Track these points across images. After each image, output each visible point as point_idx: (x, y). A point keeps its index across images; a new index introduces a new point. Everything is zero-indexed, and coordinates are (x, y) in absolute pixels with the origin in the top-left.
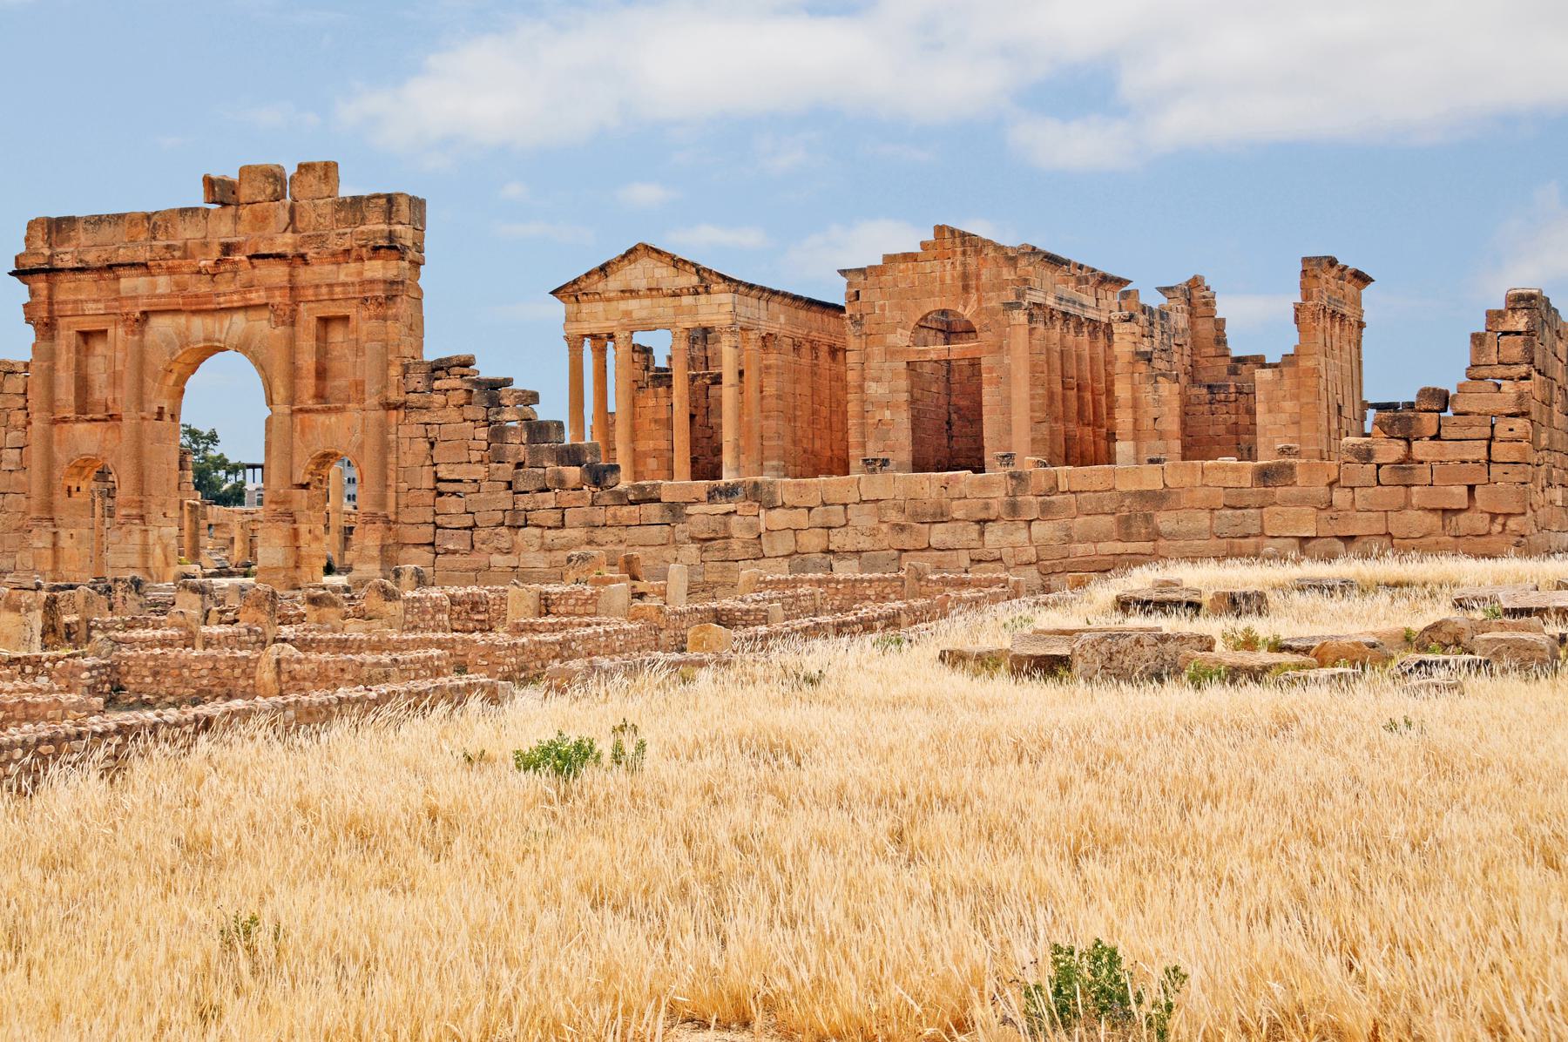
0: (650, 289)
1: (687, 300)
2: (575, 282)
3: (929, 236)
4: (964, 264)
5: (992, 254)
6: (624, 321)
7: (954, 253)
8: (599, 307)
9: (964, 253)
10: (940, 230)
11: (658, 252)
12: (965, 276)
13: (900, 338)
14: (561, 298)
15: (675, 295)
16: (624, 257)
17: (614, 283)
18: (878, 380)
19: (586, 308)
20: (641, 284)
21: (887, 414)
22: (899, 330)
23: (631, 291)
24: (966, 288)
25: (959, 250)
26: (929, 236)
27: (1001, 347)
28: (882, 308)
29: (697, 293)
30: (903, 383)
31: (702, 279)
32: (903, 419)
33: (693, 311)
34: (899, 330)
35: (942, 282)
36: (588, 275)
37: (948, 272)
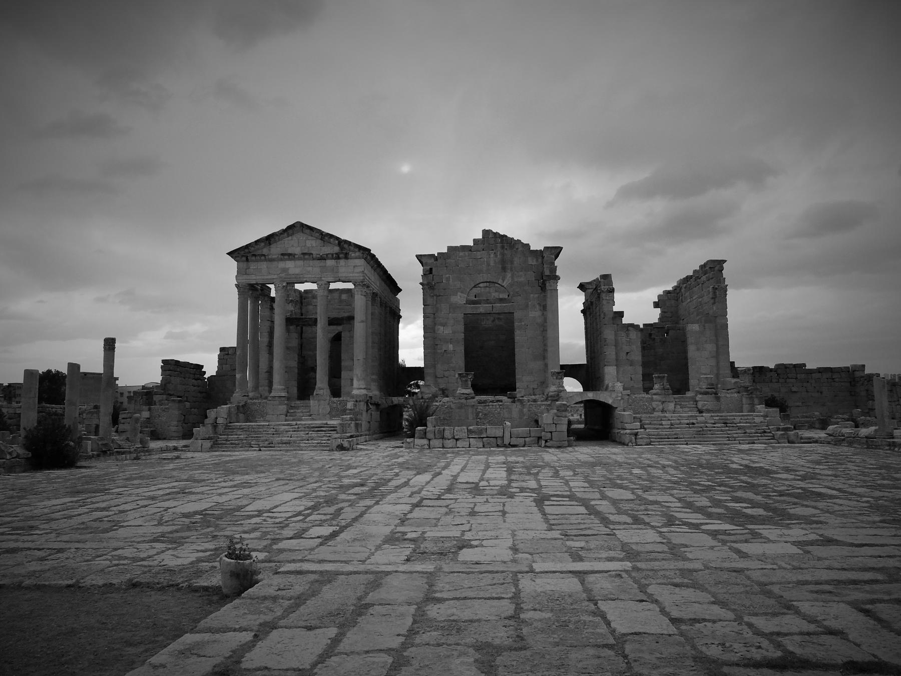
0: (304, 254)
1: (330, 263)
2: (247, 246)
4: (503, 254)
6: (283, 275)
8: (264, 266)
9: (503, 247)
10: (486, 233)
11: (311, 229)
12: (503, 262)
13: (459, 299)
14: (235, 258)
15: (322, 258)
17: (275, 250)
18: (444, 325)
19: (253, 266)
20: (297, 251)
21: (451, 347)
22: (459, 294)
23: (290, 255)
24: (504, 269)
27: (527, 306)
28: (448, 279)
29: (338, 258)
30: (461, 328)
31: (342, 248)
32: (461, 349)
34: (459, 294)
35: (488, 265)
37: (492, 259)
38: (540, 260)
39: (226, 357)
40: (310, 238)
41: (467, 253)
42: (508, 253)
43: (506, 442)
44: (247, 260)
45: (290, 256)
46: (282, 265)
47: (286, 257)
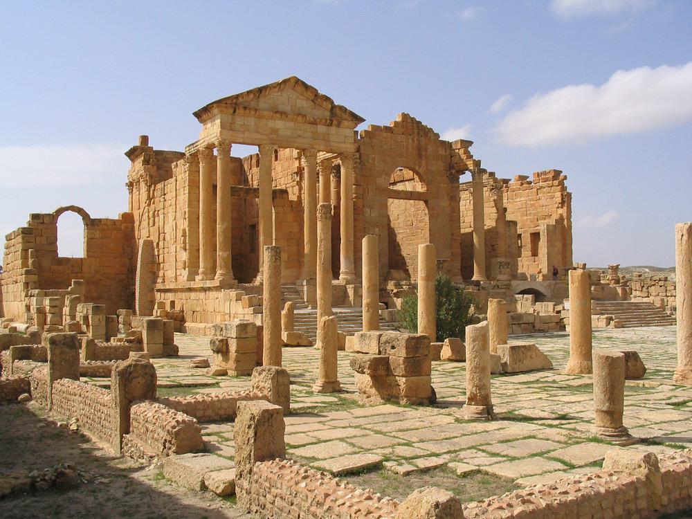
1: (321, 129)
2: (237, 97)
3: (399, 119)
4: (418, 140)
5: (433, 138)
6: (274, 136)
7: (413, 133)
9: (418, 134)
10: (405, 116)
12: (419, 149)
15: (314, 123)
16: (279, 84)
17: (264, 103)
19: (239, 121)
20: (288, 109)
22: (384, 176)
25: (416, 131)
26: (399, 119)
28: (374, 159)
33: (326, 139)
34: (384, 176)
35: (407, 150)
36: (249, 92)
38: (448, 152)
39: (40, 227)
40: (301, 97)
41: (389, 134)
42: (423, 139)
43: (537, 328)
44: (235, 111)
45: (283, 114)
46: (271, 124)
47: (278, 115)
